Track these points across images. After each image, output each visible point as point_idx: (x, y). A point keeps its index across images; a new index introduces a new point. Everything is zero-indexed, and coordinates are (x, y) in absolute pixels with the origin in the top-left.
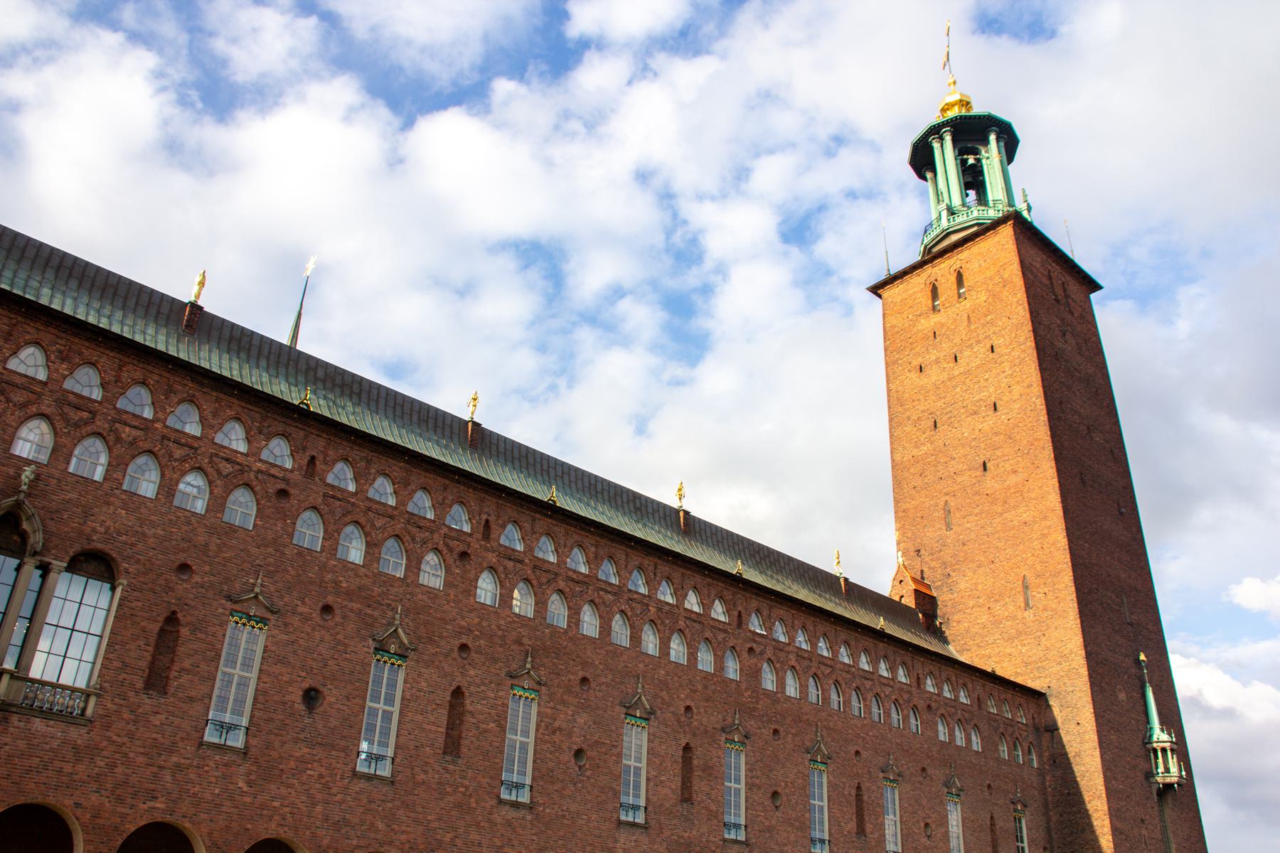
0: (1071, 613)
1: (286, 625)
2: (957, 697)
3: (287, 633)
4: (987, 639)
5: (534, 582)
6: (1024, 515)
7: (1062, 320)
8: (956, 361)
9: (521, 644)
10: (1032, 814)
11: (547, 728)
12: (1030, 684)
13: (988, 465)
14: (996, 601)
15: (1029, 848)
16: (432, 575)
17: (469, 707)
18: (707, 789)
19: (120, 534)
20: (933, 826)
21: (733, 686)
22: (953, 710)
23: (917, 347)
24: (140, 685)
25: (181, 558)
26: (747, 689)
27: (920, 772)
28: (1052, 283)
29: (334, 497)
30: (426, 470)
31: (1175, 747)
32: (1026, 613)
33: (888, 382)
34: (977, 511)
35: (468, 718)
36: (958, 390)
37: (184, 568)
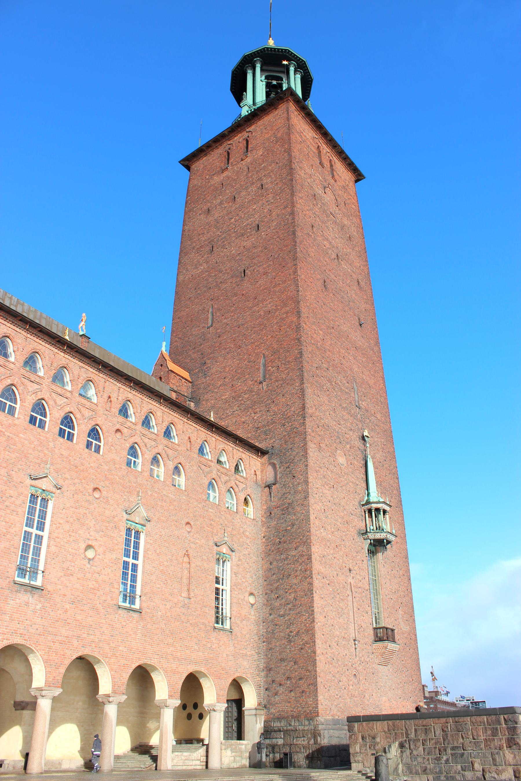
0: (297, 381)
4: (228, 412)
6: (269, 306)
10: (239, 560)
13: (246, 272)
14: (239, 378)
15: (231, 591)
22: (153, 443)
23: (209, 196)
27: (91, 491)
31: (387, 508)
33: (184, 226)
36: (233, 220)
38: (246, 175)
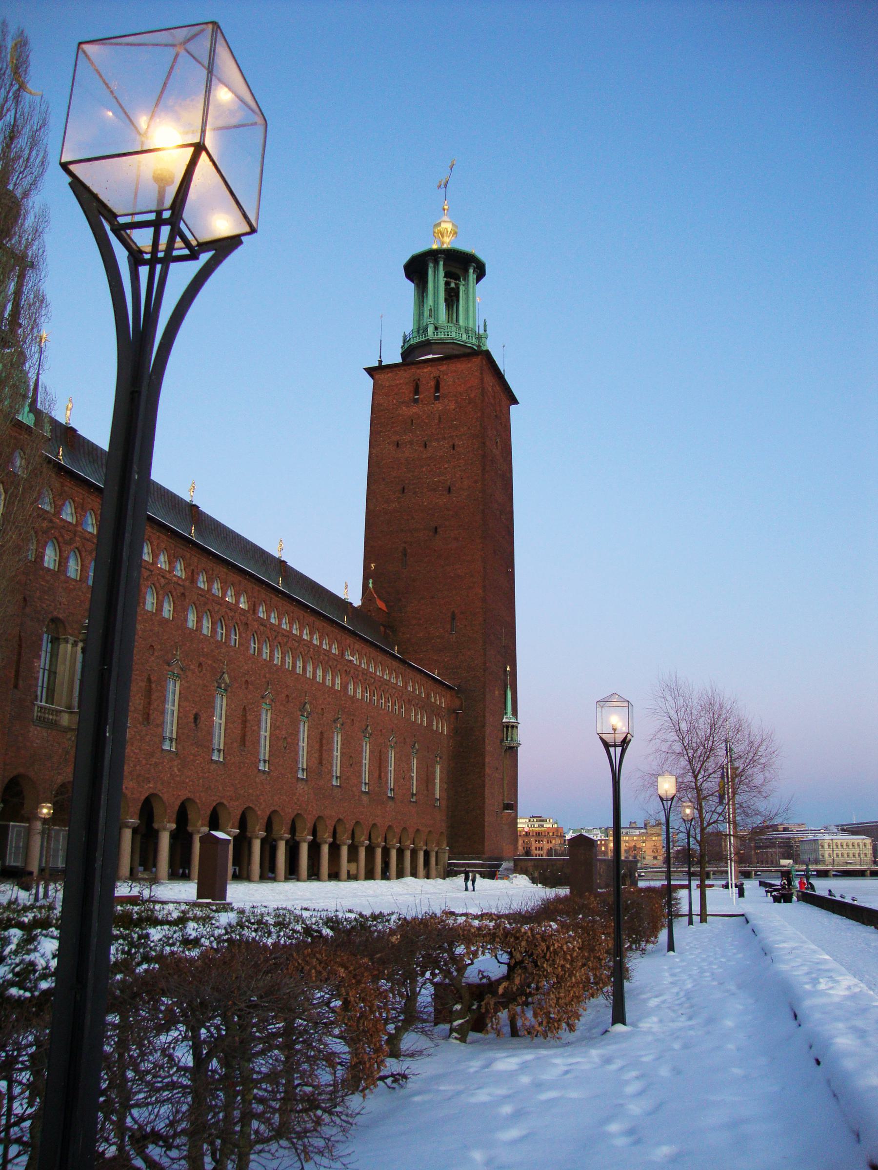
8: (426, 447)
13: (439, 530)
23: (397, 427)
30: (234, 573)
32: (451, 636)
34: (426, 560)
36: (424, 470)
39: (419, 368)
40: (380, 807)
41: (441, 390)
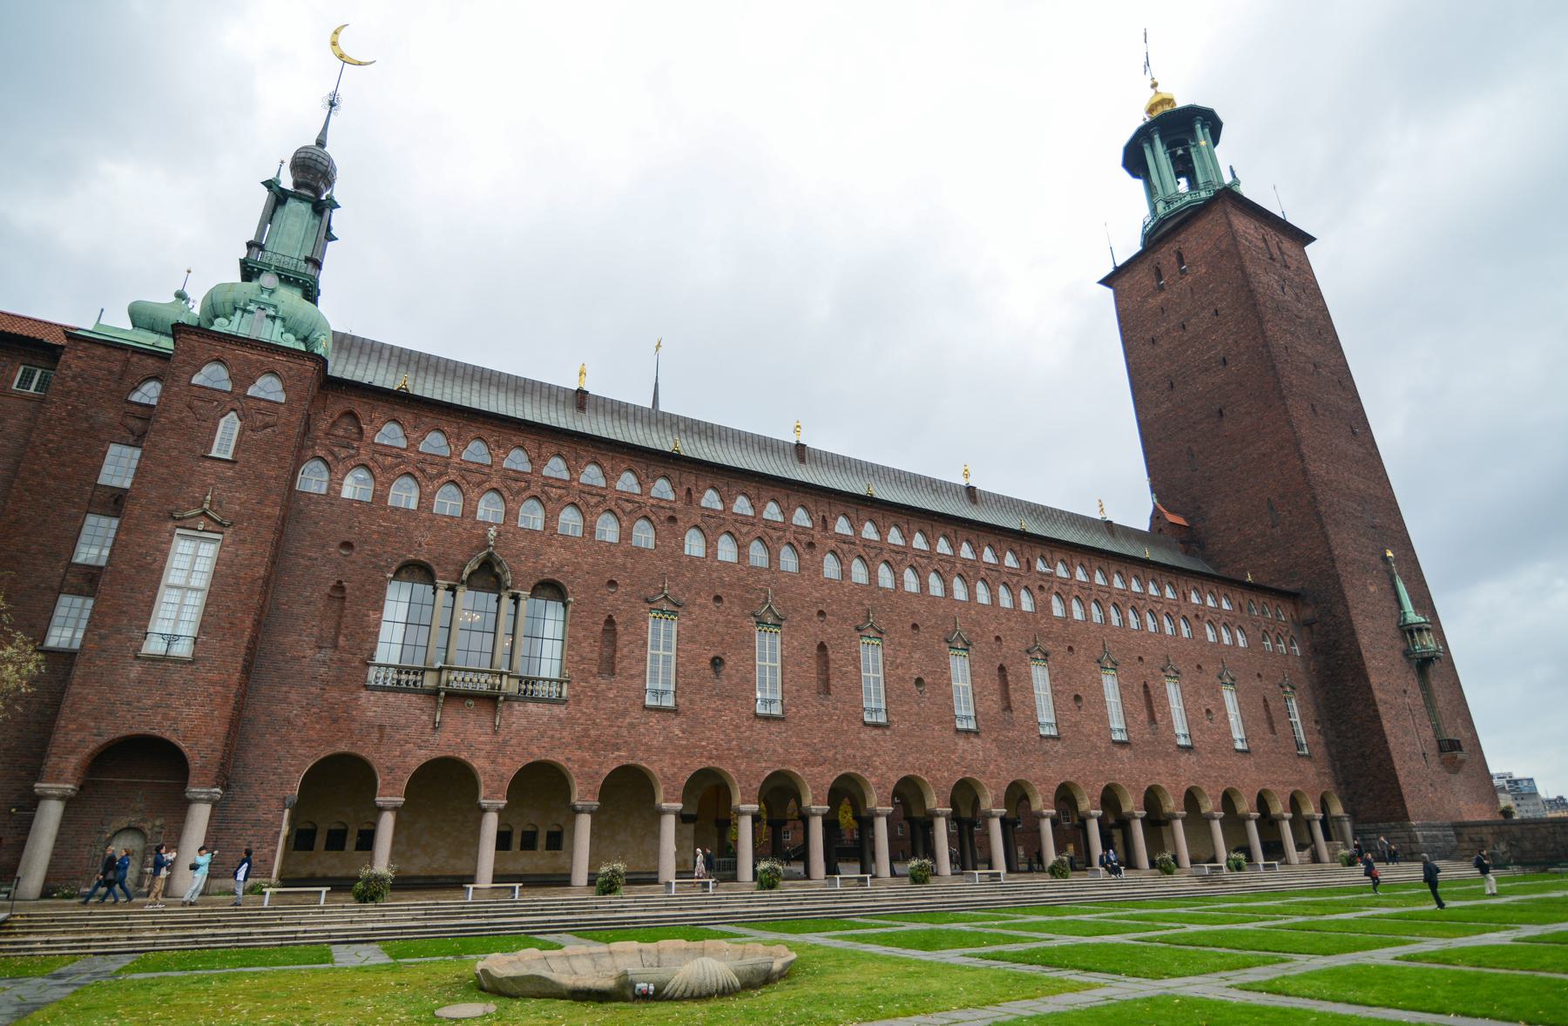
1: (690, 613)
2: (1220, 606)
3: (692, 620)
5: (866, 557)
7: (1280, 276)
9: (863, 605)
11: (890, 664)
12: (1284, 587)
13: (1224, 411)
16: (789, 561)
17: (833, 657)
18: (1021, 698)
19: (563, 566)
20: (1213, 711)
21: (1030, 617)
24: (595, 670)
25: (608, 576)
26: (1042, 618)
28: (1267, 244)
29: (708, 516)
30: (773, 486)
31: (1430, 626)
32: (1274, 530)
35: (831, 665)
37: (612, 583)
38: (1192, 297)
39: (1155, 252)
40: (1161, 762)
41: (1186, 261)
